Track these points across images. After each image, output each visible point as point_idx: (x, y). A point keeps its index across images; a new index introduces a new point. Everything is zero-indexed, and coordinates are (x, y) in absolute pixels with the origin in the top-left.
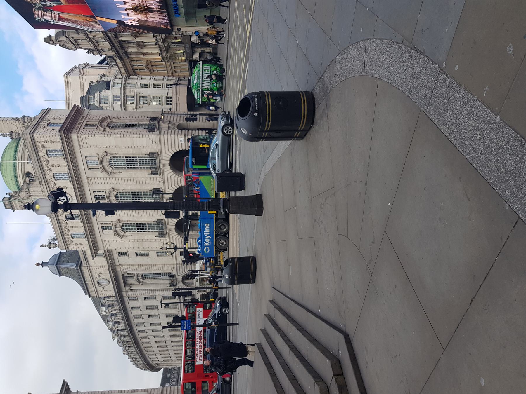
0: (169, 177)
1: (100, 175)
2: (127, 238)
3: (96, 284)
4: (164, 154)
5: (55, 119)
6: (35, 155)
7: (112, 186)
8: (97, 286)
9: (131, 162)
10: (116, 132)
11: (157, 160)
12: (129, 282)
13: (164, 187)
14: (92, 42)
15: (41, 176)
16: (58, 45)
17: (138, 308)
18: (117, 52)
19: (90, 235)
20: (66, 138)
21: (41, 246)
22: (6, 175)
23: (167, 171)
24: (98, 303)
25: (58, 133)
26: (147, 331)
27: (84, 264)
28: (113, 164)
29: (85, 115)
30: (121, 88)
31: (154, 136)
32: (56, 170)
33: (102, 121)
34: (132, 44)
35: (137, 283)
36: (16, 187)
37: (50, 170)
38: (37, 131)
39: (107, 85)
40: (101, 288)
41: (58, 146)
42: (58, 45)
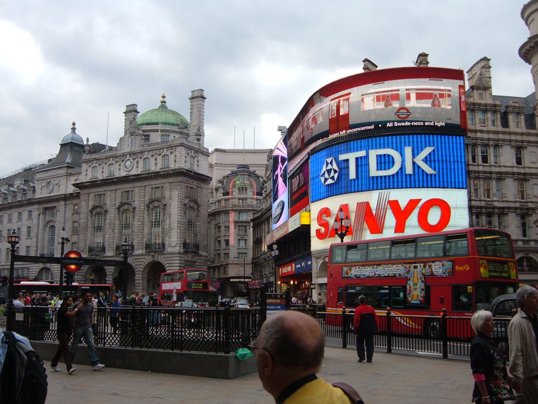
0: (143, 260)
2: (89, 217)
3: (49, 180)
4: (163, 256)
5: (198, 162)
7: (137, 207)
12: (48, 212)
13: (135, 255)
22: (152, 115)
23: (148, 259)
24: (29, 174)
27: (70, 171)
29: (202, 185)
33: (196, 202)
35: (46, 220)
36: (141, 122)
40: (44, 184)
41: (173, 166)
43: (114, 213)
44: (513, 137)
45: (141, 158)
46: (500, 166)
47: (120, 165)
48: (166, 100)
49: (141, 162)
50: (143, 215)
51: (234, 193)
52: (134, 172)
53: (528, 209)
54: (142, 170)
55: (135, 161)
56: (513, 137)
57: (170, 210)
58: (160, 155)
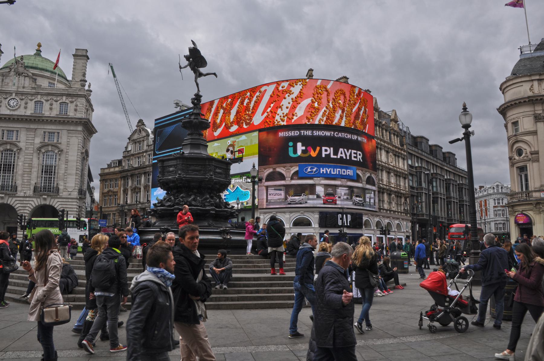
1: (38, 141)
4: (56, 200)
6: (64, 93)
7: (24, 148)
11: (52, 194)
14: (139, 153)
15: (41, 91)
16: (136, 128)
18: (128, 171)
22: (37, 60)
31: (75, 194)
32: (46, 106)
34: (136, 183)
37: (47, 101)
41: (71, 114)
42: (136, 128)
44: (386, 145)
45: (32, 100)
46: (382, 162)
48: (41, 49)
49: (31, 105)
50: (31, 157)
52: (21, 112)
53: (391, 191)
54: (33, 112)
56: (386, 145)
57: (67, 156)
58: (56, 101)
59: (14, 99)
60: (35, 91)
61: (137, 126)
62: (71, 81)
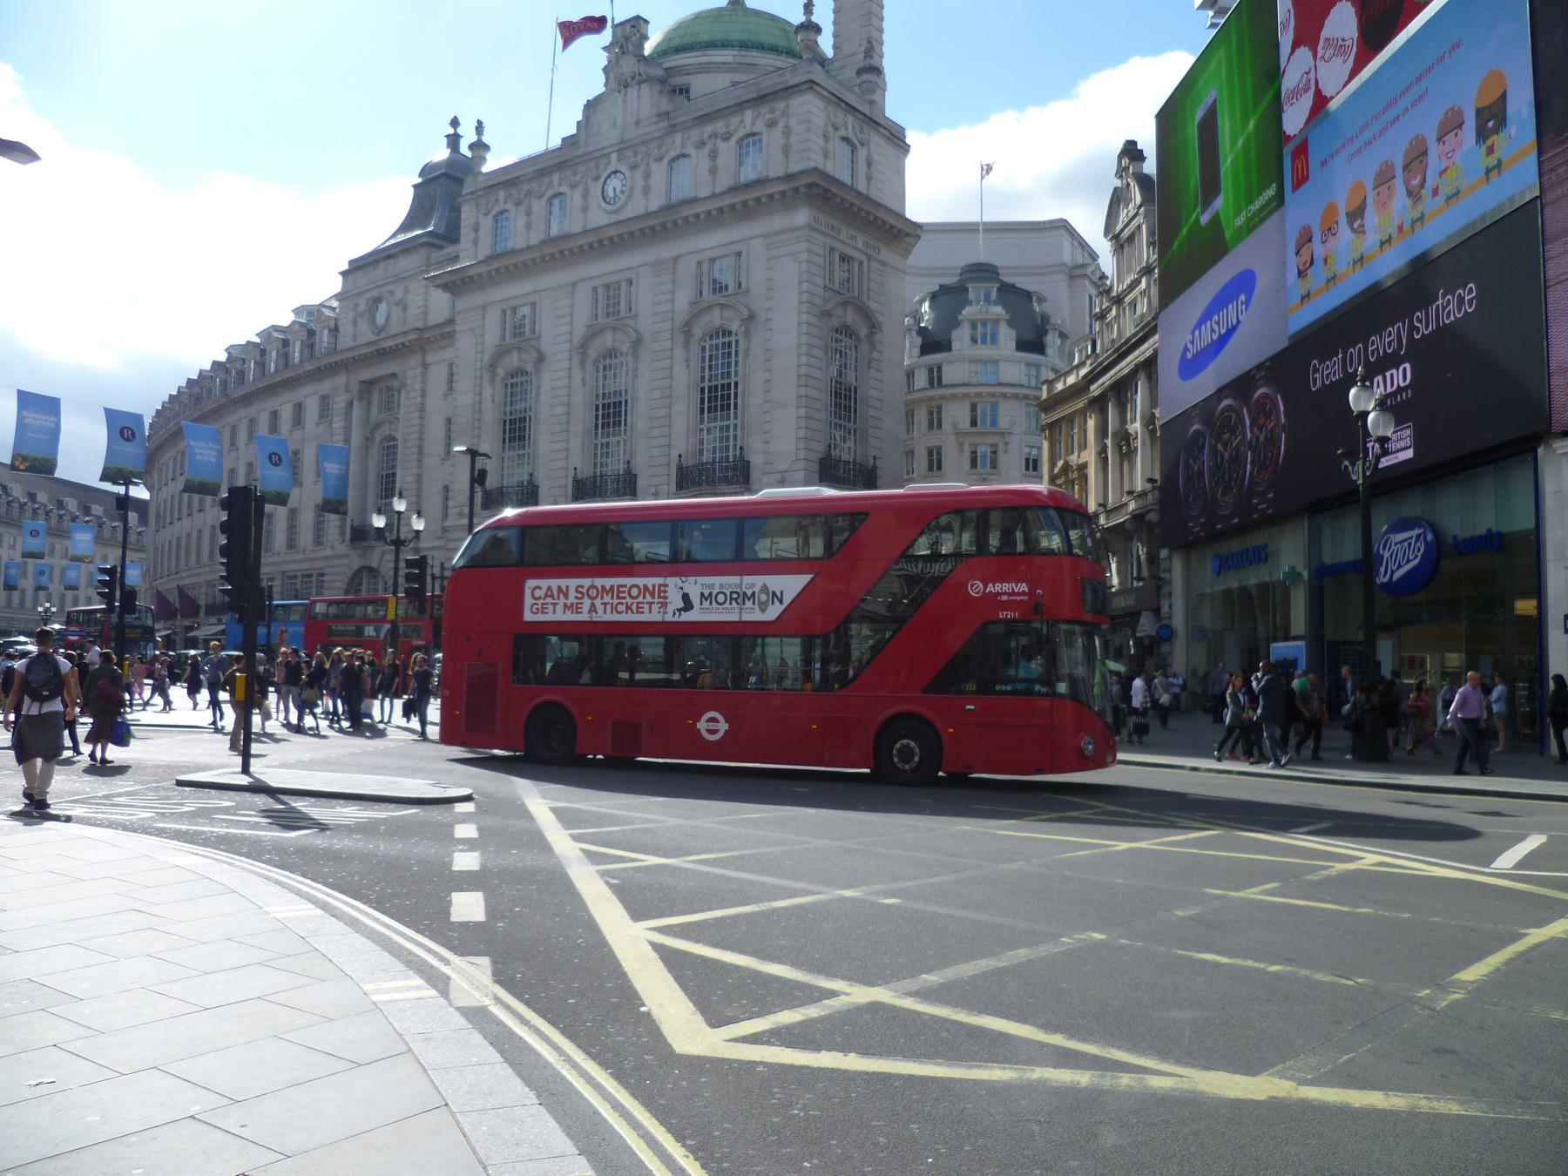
3: (375, 293)
5: (869, 164)
8: (368, 295)
9: (718, 398)
10: (819, 353)
16: (1118, 183)
17: (298, 420)
19: (498, 270)
20: (796, 189)
21: (480, 122)
25: (813, 165)
26: (234, 454)
28: (715, 342)
30: (1021, 386)
35: (372, 420)
38: (820, 104)
39: (1032, 343)
43: (566, 365)
47: (585, 196)
51: (955, 345)
55: (639, 173)
58: (727, 138)
59: (615, 172)
60: (665, 124)
61: (1121, 172)
62: (832, 61)
